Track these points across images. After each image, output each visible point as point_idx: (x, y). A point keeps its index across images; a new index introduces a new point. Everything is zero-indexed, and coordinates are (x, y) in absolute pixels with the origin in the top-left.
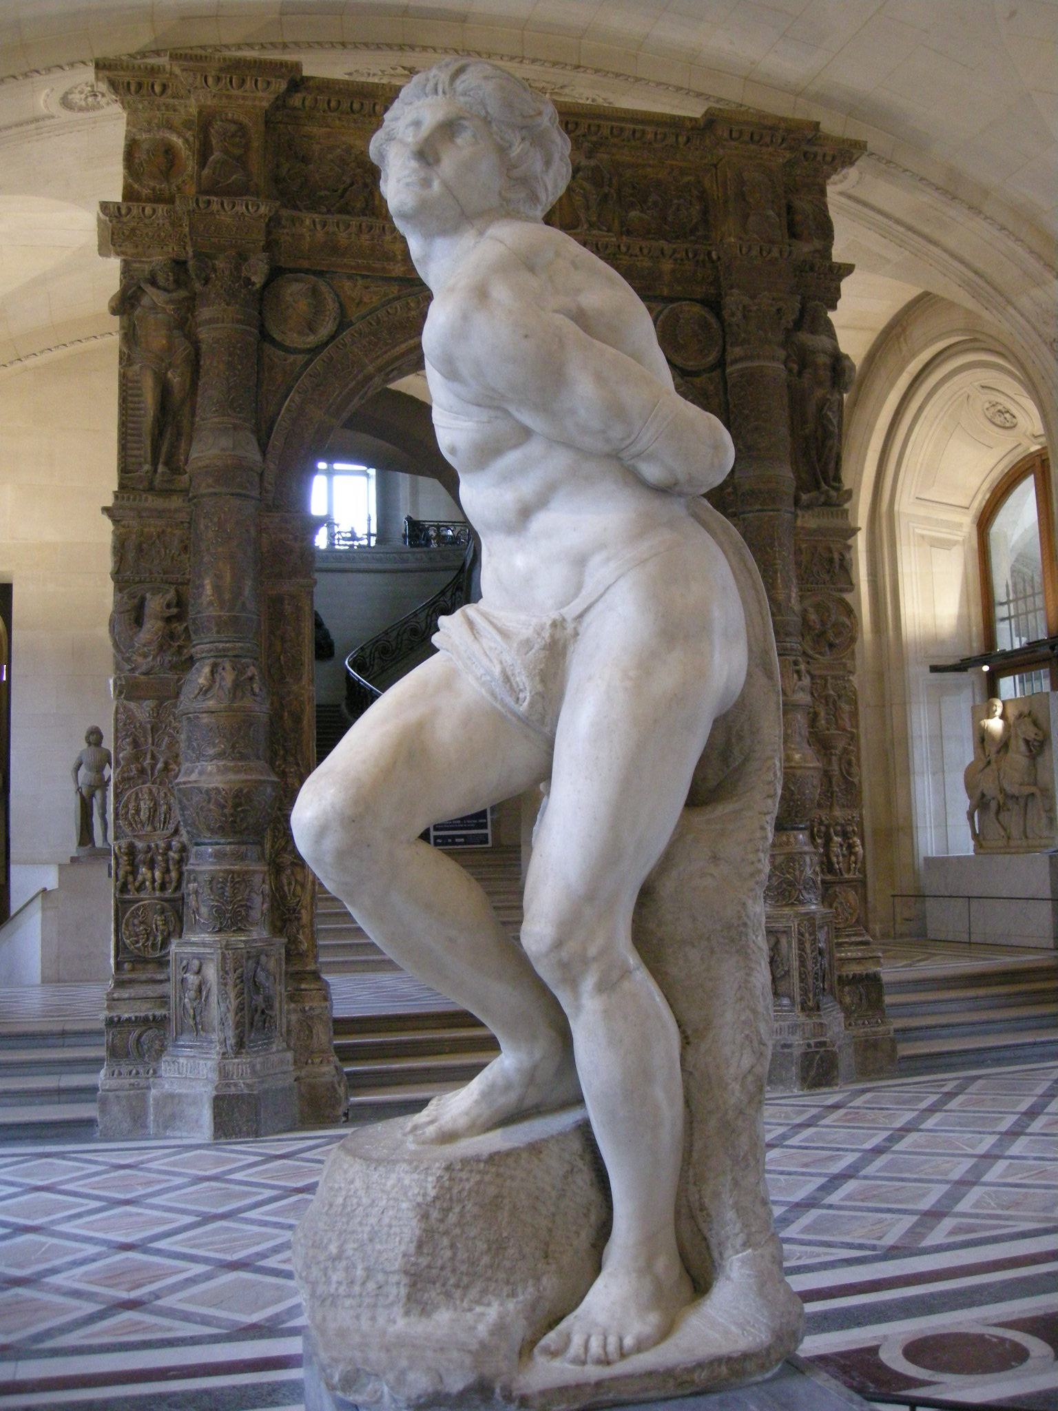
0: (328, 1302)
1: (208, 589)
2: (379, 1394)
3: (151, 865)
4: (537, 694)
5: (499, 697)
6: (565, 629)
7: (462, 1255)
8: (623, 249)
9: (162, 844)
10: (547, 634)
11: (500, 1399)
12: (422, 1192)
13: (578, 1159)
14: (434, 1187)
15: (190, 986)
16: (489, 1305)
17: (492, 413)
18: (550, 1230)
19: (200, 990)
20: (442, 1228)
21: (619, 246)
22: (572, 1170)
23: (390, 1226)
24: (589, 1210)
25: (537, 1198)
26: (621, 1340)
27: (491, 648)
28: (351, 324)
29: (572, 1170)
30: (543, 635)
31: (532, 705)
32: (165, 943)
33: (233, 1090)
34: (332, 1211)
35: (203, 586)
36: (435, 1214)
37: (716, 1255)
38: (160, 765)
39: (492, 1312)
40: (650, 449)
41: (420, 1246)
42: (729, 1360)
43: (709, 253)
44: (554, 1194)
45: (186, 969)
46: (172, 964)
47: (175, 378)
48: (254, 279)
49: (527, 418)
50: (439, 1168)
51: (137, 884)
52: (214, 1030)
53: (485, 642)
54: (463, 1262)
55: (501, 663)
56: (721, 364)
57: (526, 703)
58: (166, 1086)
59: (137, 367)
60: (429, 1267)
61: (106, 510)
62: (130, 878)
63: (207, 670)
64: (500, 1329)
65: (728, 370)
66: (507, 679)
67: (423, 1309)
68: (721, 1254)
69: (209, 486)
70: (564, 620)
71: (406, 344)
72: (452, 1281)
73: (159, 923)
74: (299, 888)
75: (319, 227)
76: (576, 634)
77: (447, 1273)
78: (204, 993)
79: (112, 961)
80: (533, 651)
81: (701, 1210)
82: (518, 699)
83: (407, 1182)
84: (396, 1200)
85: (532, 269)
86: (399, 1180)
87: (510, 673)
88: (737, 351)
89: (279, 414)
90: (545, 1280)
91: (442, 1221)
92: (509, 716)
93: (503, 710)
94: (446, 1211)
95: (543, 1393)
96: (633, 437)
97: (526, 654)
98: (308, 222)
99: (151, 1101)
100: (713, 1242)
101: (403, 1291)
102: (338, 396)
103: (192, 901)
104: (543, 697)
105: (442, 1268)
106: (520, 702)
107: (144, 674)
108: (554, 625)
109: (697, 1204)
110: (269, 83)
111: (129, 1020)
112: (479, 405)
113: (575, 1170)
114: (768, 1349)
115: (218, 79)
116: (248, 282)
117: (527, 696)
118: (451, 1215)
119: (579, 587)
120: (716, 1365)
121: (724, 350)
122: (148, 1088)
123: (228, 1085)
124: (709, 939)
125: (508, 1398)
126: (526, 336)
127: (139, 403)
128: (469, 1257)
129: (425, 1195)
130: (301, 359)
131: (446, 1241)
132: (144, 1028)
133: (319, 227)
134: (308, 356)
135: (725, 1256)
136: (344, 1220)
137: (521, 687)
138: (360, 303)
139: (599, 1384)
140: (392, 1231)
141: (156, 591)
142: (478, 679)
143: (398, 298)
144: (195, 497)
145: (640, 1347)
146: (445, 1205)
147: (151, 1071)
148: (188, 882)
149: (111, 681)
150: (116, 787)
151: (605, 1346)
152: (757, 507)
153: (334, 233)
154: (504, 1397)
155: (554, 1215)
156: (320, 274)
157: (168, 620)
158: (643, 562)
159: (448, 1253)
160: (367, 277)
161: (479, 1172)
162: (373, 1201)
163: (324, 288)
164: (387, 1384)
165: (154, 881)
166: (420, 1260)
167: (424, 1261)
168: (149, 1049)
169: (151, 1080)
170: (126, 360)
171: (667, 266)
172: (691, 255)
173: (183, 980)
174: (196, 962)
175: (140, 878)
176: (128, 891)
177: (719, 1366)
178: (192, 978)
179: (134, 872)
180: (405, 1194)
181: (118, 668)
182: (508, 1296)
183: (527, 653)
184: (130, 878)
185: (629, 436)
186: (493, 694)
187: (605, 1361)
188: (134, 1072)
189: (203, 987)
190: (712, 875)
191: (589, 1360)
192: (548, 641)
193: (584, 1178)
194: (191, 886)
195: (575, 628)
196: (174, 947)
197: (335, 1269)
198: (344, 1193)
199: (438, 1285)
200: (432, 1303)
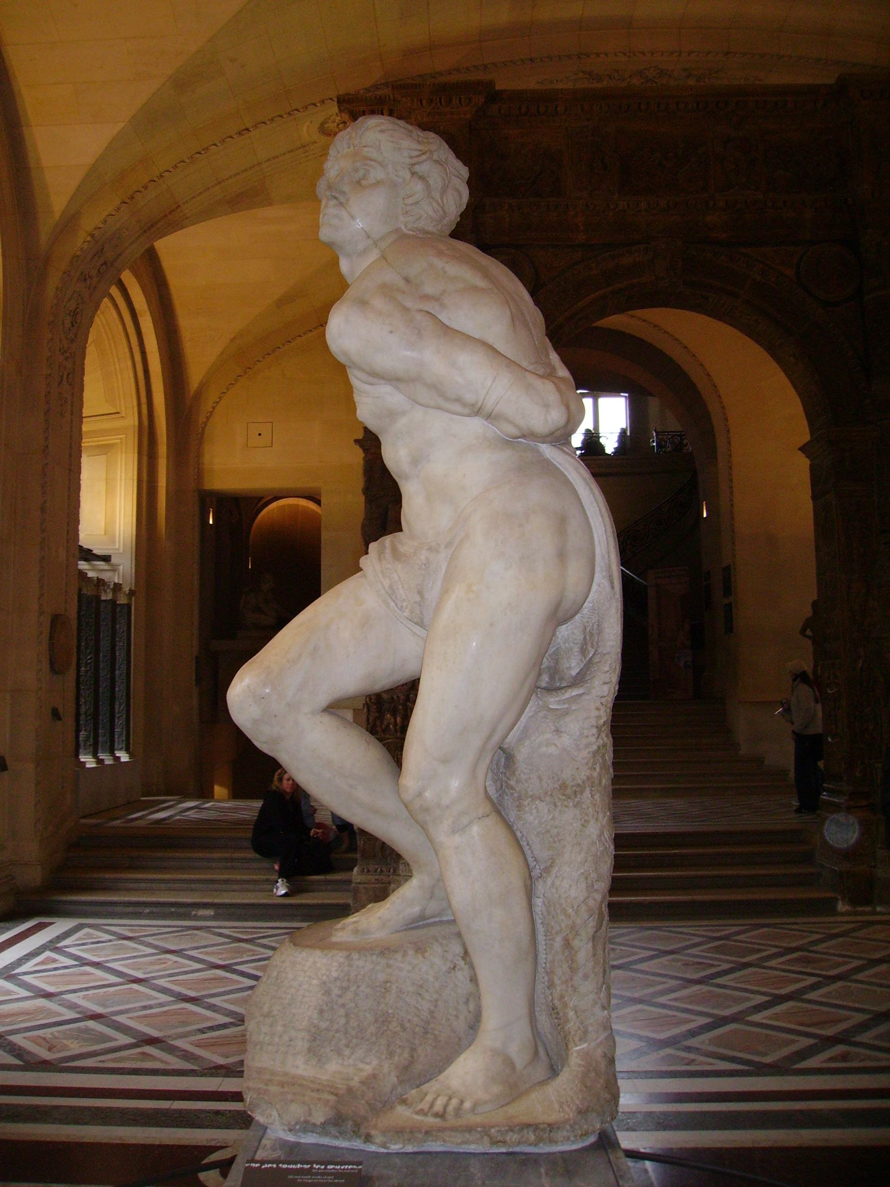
0: (258, 1047)
3: (394, 713)
7: (353, 1023)
9: (402, 697)
12: (327, 973)
13: (460, 959)
14: (336, 971)
18: (431, 1013)
20: (341, 1001)
22: (454, 968)
23: (304, 996)
24: (468, 1000)
25: (421, 986)
29: (454, 968)
36: (336, 991)
44: (437, 985)
50: (342, 956)
51: (383, 727)
54: (353, 1028)
60: (327, 1029)
61: (357, 441)
67: (319, 1060)
72: (344, 1042)
84: (310, 977)
86: (315, 963)
91: (340, 996)
94: (345, 989)
101: (306, 1045)
105: (337, 1031)
110: (470, 99)
113: (458, 967)
115: (431, 101)
122: (389, 883)
128: (358, 1025)
131: (342, 1012)
136: (276, 988)
140: (304, 1000)
147: (392, 870)
155: (436, 1001)
159: (343, 1021)
161: (373, 962)
165: (395, 724)
166: (321, 1023)
167: (323, 1025)
169: (391, 877)
175: (385, 722)
179: (381, 717)
184: (378, 723)
187: (442, 1115)
190: (555, 745)
199: (333, 1043)
200: (326, 1056)
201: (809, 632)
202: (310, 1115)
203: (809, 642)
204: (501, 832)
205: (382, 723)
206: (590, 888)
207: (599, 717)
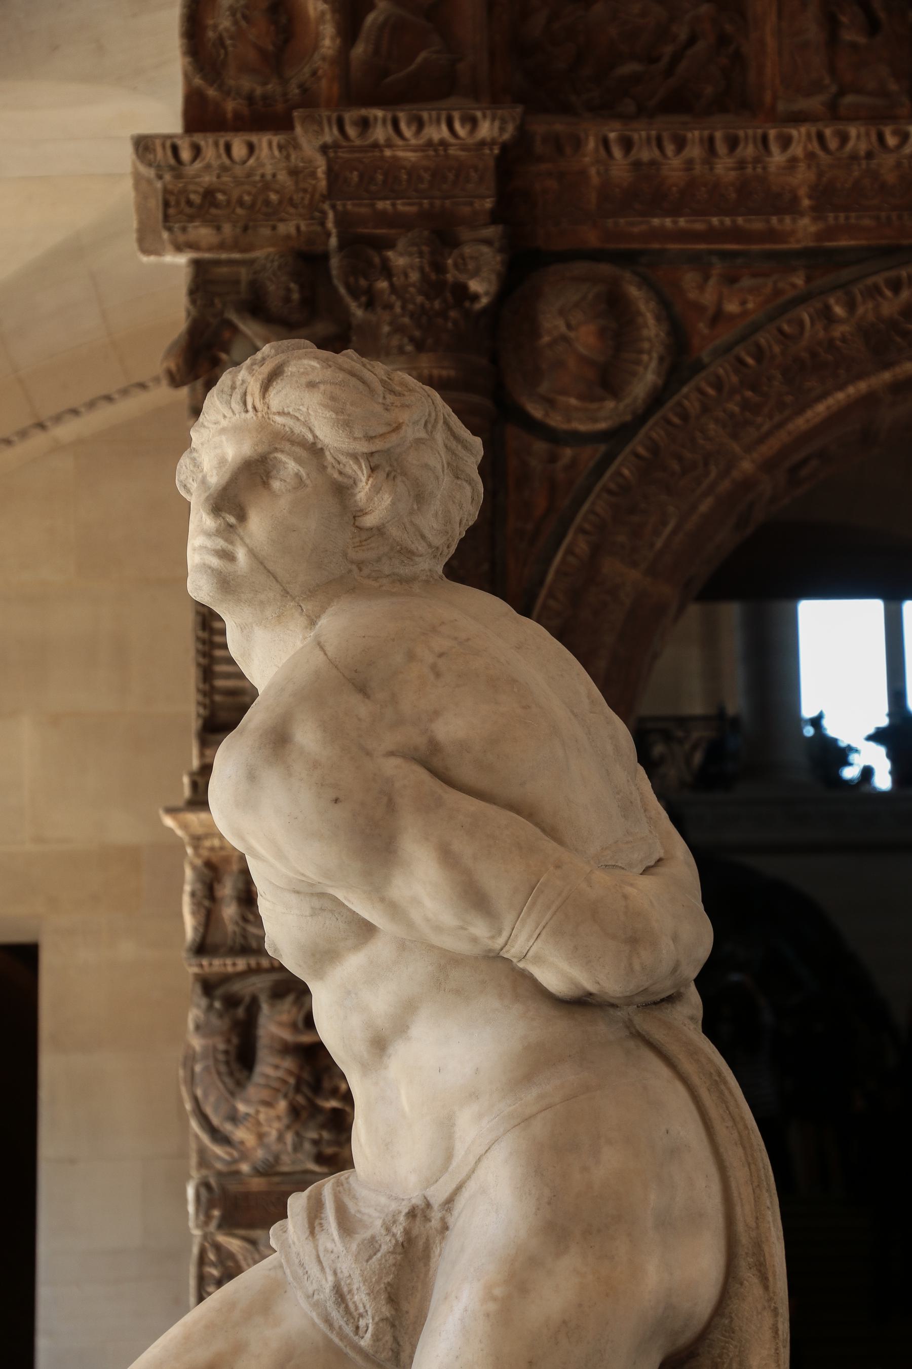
4: (382, 1320)
5: (336, 1325)
6: (427, 1219)
10: (398, 1230)
17: (316, 903)
27: (326, 1250)
28: (699, 367)
30: (394, 1230)
31: (376, 1338)
48: (475, 286)
53: (323, 1240)
55: (335, 1273)
57: (368, 1335)
66: (340, 1295)
70: (428, 1205)
71: (830, 401)
75: (617, 152)
76: (445, 1227)
80: (379, 1255)
82: (357, 1328)
85: (363, 690)
87: (345, 1289)
89: (541, 582)
92: (352, 1354)
93: (341, 1344)
96: (505, 934)
97: (367, 1261)
102: (674, 532)
104: (393, 1326)
106: (361, 1333)
107: (258, 1172)
108: (412, 1214)
112: (298, 892)
116: (462, 293)
117: (368, 1322)
119: (449, 1155)
126: (336, 801)
130: (590, 455)
133: (617, 152)
134: (603, 448)
137: (361, 1310)
138: (718, 317)
142: (309, 1297)
143: (802, 299)
149: (190, 1192)
153: (653, 163)
156: (626, 259)
158: (527, 1120)
160: (734, 255)
163: (635, 292)
181: (204, 1161)
183: (370, 1258)
185: (500, 933)
186: (328, 1321)
192: (401, 1240)
195: (443, 1220)
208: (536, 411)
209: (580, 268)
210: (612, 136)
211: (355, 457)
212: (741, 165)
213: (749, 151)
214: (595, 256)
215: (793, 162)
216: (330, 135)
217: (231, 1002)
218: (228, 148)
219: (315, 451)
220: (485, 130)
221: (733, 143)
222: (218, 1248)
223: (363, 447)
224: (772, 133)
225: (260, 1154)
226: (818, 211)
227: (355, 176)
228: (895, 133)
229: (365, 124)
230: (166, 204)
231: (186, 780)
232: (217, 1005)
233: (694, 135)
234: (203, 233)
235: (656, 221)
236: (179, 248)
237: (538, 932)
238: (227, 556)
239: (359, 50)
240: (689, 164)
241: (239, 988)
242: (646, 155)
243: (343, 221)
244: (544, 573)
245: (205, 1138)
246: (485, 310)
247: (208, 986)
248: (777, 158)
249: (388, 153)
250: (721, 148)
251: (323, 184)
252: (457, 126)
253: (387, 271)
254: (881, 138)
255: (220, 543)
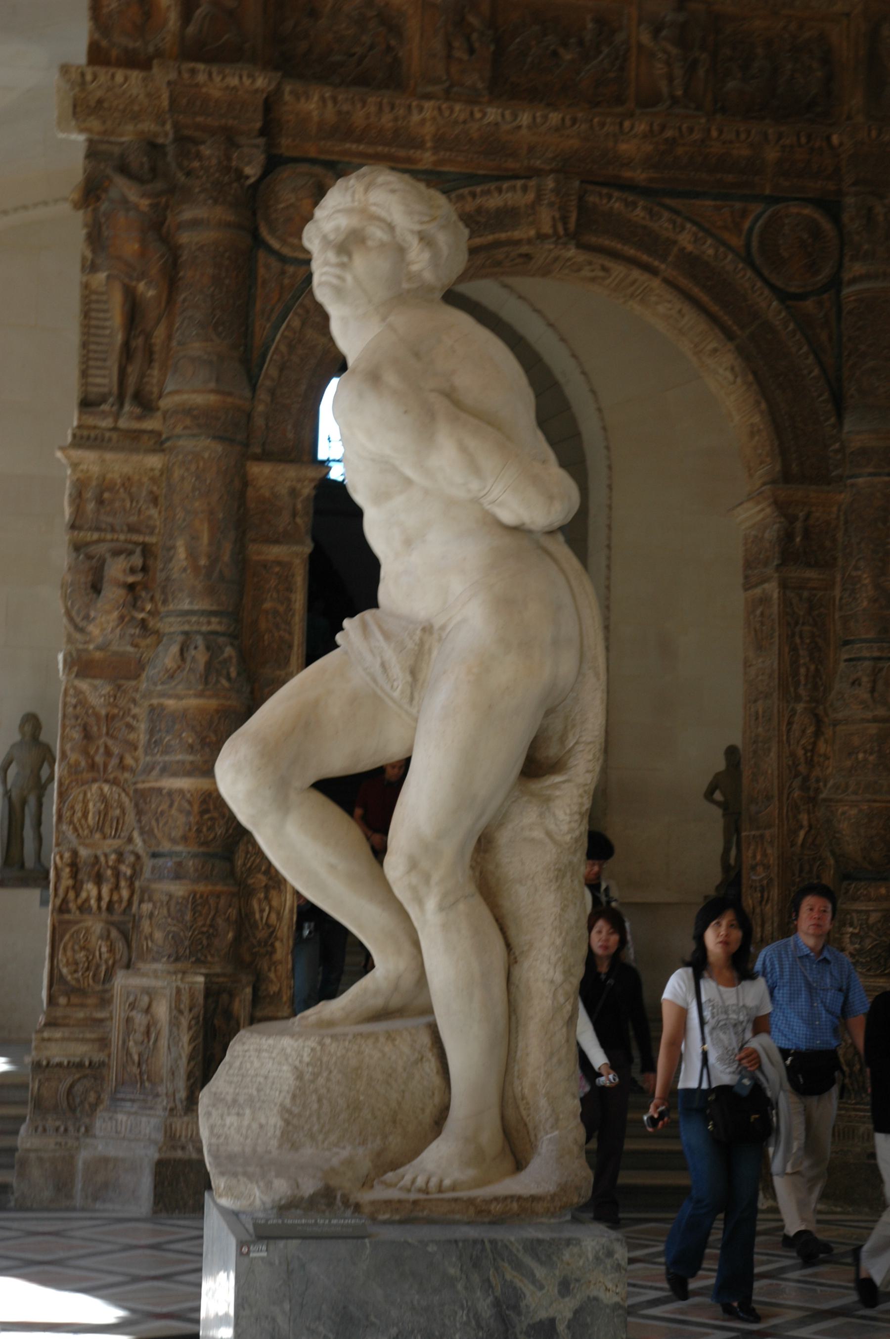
1: (181, 553)
2: (252, 1198)
3: (99, 880)
8: (714, 134)
11: (340, 1204)
15: (136, 1027)
16: (344, 1148)
18: (399, 1103)
19: (148, 1033)
21: (709, 130)
24: (433, 1094)
25: (390, 1075)
26: (441, 1181)
31: (402, 692)
32: (109, 975)
33: (179, 1154)
34: (231, 1072)
35: (173, 547)
36: (307, 1077)
37: (533, 1138)
38: (114, 762)
39: (345, 1154)
40: (500, 499)
41: (294, 1097)
42: (519, 1198)
43: (828, 138)
45: (132, 1006)
46: (117, 1000)
47: (147, 291)
48: (248, 170)
49: (409, 472)
51: (80, 901)
52: (162, 1080)
55: (382, 657)
56: (835, 283)
58: (100, 1148)
59: (102, 276)
62: (71, 895)
63: (175, 649)
64: (349, 1162)
65: (846, 291)
68: (536, 1136)
69: (185, 428)
73: (104, 949)
74: (273, 916)
77: (315, 1119)
78: (153, 1036)
79: (44, 994)
81: (523, 1099)
83: (289, 1051)
88: (858, 268)
89: (273, 340)
90: (391, 1138)
91: (313, 1081)
94: (316, 1076)
95: (373, 1203)
98: (316, 98)
99: (80, 1165)
100: (530, 1126)
103: (146, 926)
109: (520, 1095)
111: (60, 1065)
113: (424, 1059)
114: (553, 1197)
116: (240, 176)
118: (320, 1078)
120: (509, 1200)
121: (840, 266)
123: (174, 1148)
124: (533, 879)
125: (346, 1203)
126: (406, 412)
127: (106, 320)
129: (301, 1062)
131: (314, 1097)
132: (77, 1076)
133: (330, 104)
135: (539, 1137)
139: (415, 1202)
141: (116, 553)
144: (168, 439)
145: (453, 1188)
146: (316, 1070)
147: (83, 1129)
148: (141, 901)
149: (60, 657)
150: (61, 784)
151: (428, 1182)
152: (869, 470)
153: (348, 113)
154: (343, 1203)
155: (403, 1092)
157: (131, 587)
162: (262, 1064)
164: (259, 1187)
165: (99, 898)
166: (293, 1108)
168: (82, 1102)
170: (90, 267)
171: (772, 155)
172: (803, 140)
173: (129, 1020)
174: (146, 999)
175: (84, 895)
176: (68, 911)
177: (512, 1201)
178: (140, 1019)
179: (77, 887)
180: (287, 1059)
181: (70, 640)
182: (359, 1144)
184: (71, 895)
188: (62, 1129)
189: (152, 1029)
191: (413, 1189)
193: (431, 1065)
194: (146, 907)
196: (121, 981)
197: (229, 1114)
198: (240, 1059)
201: (718, 796)
202: (298, 1186)
203: (718, 812)
204: (484, 911)
205: (77, 895)
206: (567, 973)
207: (581, 805)
208: (275, 244)
209: (304, 168)
210: (327, 95)
211: (412, 232)
212: (396, 119)
213: (401, 112)
214: (313, 161)
215: (423, 122)
216: (173, 76)
217: (89, 557)
218: (113, 76)
219: (391, 228)
220: (261, 82)
221: (393, 107)
222: (75, 688)
223: (417, 227)
224: (414, 104)
225: (100, 640)
226: (436, 149)
227: (184, 101)
228: (481, 111)
229: (193, 72)
230: (75, 106)
231: (69, 433)
232: (82, 557)
233: (372, 100)
234: (95, 124)
235: (348, 146)
236: (81, 130)
237: (505, 489)
238: (341, 278)
239: (191, 29)
240: (368, 116)
241: (93, 549)
242: (346, 107)
243: (176, 126)
244: (275, 336)
245: (71, 629)
246: (251, 186)
247: (77, 547)
248: (416, 118)
249: (204, 90)
250: (387, 109)
251: (165, 103)
252: (245, 78)
253: (199, 156)
254: (472, 114)
255: (337, 271)
